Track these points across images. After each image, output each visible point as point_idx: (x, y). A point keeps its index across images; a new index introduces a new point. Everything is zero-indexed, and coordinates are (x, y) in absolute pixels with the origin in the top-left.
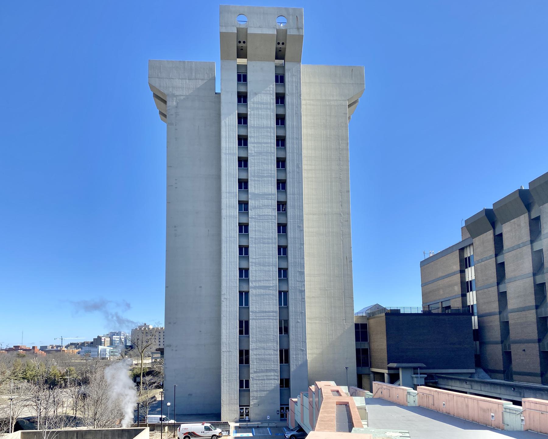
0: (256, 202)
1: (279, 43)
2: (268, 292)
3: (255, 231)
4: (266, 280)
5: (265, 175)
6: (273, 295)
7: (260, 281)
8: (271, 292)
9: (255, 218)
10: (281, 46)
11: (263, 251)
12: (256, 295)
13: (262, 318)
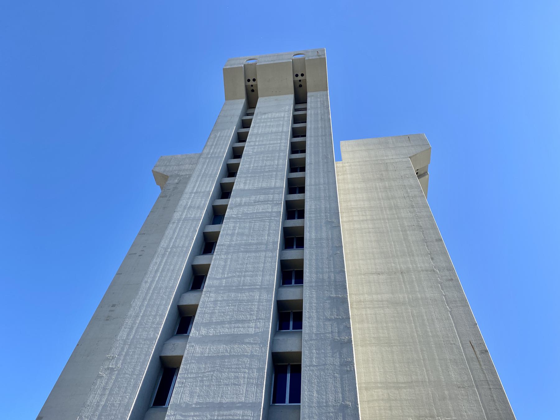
1: (297, 75)
2: (237, 348)
3: (232, 235)
4: (238, 321)
5: (267, 170)
6: (252, 356)
7: (222, 323)
8: (248, 349)
9: (237, 218)
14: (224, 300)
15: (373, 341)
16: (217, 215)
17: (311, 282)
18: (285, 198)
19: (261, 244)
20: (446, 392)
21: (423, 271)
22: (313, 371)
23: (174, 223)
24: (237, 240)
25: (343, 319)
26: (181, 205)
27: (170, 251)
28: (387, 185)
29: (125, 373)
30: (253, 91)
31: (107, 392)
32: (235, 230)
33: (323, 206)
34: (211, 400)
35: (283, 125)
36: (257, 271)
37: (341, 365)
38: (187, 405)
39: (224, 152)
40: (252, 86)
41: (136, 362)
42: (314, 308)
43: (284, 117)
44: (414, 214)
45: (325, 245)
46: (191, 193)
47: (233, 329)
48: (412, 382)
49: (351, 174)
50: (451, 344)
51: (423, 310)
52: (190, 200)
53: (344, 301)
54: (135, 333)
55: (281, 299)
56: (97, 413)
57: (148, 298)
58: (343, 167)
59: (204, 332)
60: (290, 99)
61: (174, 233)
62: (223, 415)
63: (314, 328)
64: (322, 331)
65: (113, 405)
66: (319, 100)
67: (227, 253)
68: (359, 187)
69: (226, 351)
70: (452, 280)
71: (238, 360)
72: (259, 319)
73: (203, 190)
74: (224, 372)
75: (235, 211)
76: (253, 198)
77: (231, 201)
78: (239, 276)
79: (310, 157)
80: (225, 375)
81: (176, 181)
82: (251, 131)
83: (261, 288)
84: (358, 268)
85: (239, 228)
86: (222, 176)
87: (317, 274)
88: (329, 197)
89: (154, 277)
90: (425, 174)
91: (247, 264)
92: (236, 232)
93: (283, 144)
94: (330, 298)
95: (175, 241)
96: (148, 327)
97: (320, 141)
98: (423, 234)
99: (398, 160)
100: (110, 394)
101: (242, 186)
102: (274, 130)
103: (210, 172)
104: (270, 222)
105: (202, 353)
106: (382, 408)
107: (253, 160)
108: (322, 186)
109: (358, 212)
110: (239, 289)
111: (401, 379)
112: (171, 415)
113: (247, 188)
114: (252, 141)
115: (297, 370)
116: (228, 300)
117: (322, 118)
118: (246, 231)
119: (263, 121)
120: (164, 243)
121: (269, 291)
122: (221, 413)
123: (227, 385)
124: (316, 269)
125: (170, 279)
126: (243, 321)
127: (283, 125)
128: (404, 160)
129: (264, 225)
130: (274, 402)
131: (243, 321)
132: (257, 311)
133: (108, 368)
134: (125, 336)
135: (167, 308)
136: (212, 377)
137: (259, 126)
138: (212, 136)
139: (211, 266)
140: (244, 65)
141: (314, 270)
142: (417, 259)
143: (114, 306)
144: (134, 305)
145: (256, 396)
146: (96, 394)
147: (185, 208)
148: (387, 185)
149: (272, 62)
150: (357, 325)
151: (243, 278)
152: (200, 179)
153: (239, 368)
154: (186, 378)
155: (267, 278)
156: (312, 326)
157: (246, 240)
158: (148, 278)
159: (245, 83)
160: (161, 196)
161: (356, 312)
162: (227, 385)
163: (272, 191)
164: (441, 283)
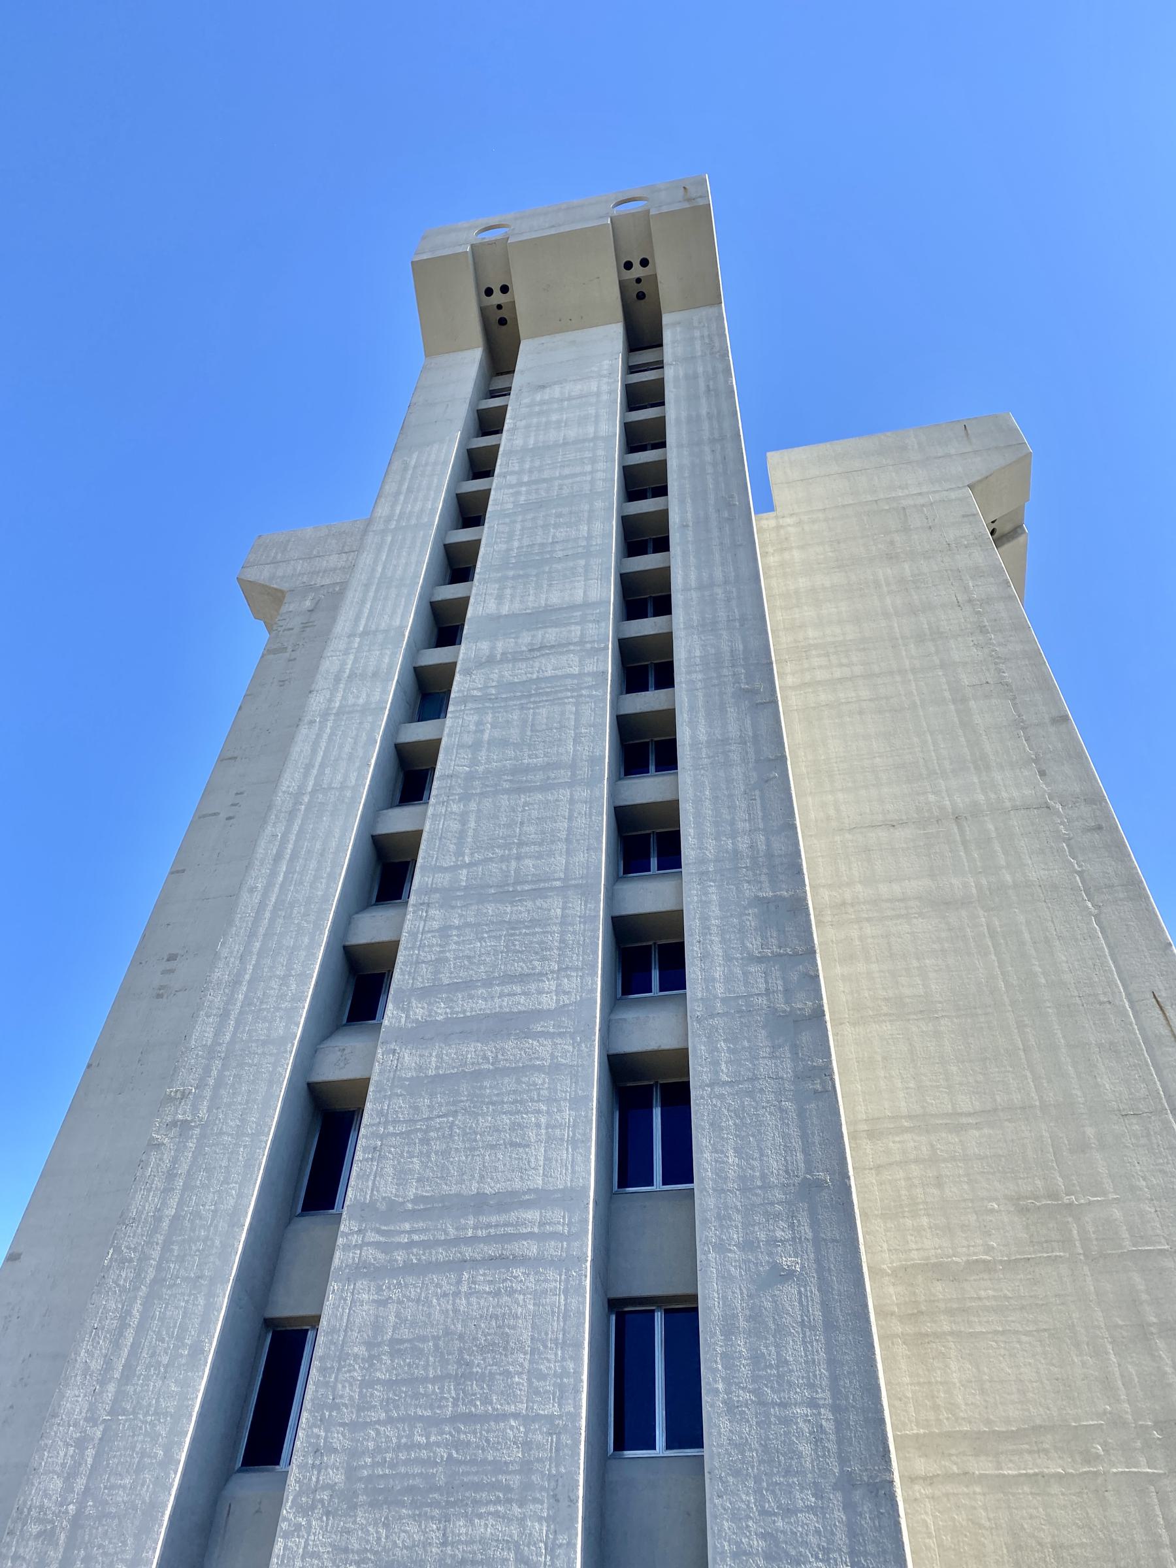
0: (500, 645)
1: (628, 265)
3: (476, 746)
5: (560, 554)
7: (467, 985)
8: (543, 1049)
10: (637, 271)
11: (508, 826)
12: (421, 1084)
13: (441, 1254)
14: (467, 925)
15: (885, 1009)
16: (428, 694)
17: (702, 861)
18: (617, 629)
19: (557, 766)
20: (1090, 1131)
21: (1016, 808)
22: (721, 1097)
23: (312, 722)
24: (488, 761)
25: (796, 954)
26: (327, 672)
27: (309, 802)
28: (908, 572)
29: (221, 1133)
30: (503, 321)
31: (179, 1183)
32: (482, 731)
33: (725, 648)
34: (454, 1189)
35: (597, 416)
36: (553, 842)
37: (798, 1077)
38: (391, 1204)
39: (433, 510)
40: (499, 307)
41: (247, 1102)
42: (714, 930)
43: (598, 394)
44: (986, 651)
45: (735, 757)
46: (351, 635)
47: (496, 1000)
48: (995, 1110)
49: (802, 547)
50: (1101, 1003)
51: (1021, 918)
52: (352, 657)
53: (798, 907)
54: (236, 1028)
55: (624, 913)
56: (160, 1238)
57: (262, 931)
58: (779, 527)
59: (419, 1011)
60: (614, 335)
61: (314, 751)
62: (489, 1226)
63: (717, 985)
64: (741, 990)
65: (197, 1214)
66: (697, 334)
67: (465, 798)
68: (828, 584)
69: (485, 1058)
70: (1100, 828)
71: (519, 1082)
72: (567, 968)
73: (383, 626)
74: (483, 1115)
75: (478, 678)
76: (526, 639)
77: (465, 652)
78: (503, 859)
79: (680, 508)
80: (484, 1122)
81: (308, 604)
82: (507, 441)
83: (565, 888)
84: (832, 812)
85: (493, 726)
86: (432, 583)
87: (717, 838)
88: (743, 620)
89: (273, 874)
90: (1016, 531)
91: (522, 823)
92: (486, 737)
93: (600, 475)
94: (759, 901)
95: (321, 772)
96: (268, 1010)
97: (708, 458)
98: (1015, 705)
99: (937, 497)
100: (186, 1187)
101: (491, 606)
102: (572, 433)
103: (399, 572)
104: (577, 704)
105: (420, 1068)
106: (916, 1182)
107: (518, 526)
108: (719, 591)
109: (827, 655)
110: (507, 893)
111: (965, 1103)
112: (352, 1233)
113: (505, 610)
114: (513, 473)
115: (678, 1097)
116: (479, 924)
117: (708, 389)
118: (514, 734)
119: (537, 409)
120: (289, 782)
121: (586, 892)
122: (484, 1219)
123: (493, 1147)
124: (716, 824)
125: (316, 878)
126: (522, 978)
127: (597, 416)
128: (953, 495)
129: (563, 713)
130: (623, 1183)
131: (522, 978)
132: (559, 949)
133: (174, 1123)
134: (211, 1035)
135: (314, 955)
136: (451, 1128)
137: (528, 427)
138: (397, 465)
139: (425, 836)
140: (472, 246)
141: (708, 828)
142: (998, 777)
143: (172, 958)
144: (225, 952)
145: (573, 1172)
146: (149, 1190)
147: (337, 679)
148: (908, 572)
149: (553, 232)
150: (838, 970)
151: (513, 864)
152: (371, 594)
153: (522, 1102)
154: (382, 1137)
155: (581, 857)
156: (714, 980)
157: (516, 758)
158: (257, 878)
159: (479, 301)
160: (269, 651)
161: (831, 933)
162: (493, 1147)
163: (578, 614)
164: (1068, 840)
